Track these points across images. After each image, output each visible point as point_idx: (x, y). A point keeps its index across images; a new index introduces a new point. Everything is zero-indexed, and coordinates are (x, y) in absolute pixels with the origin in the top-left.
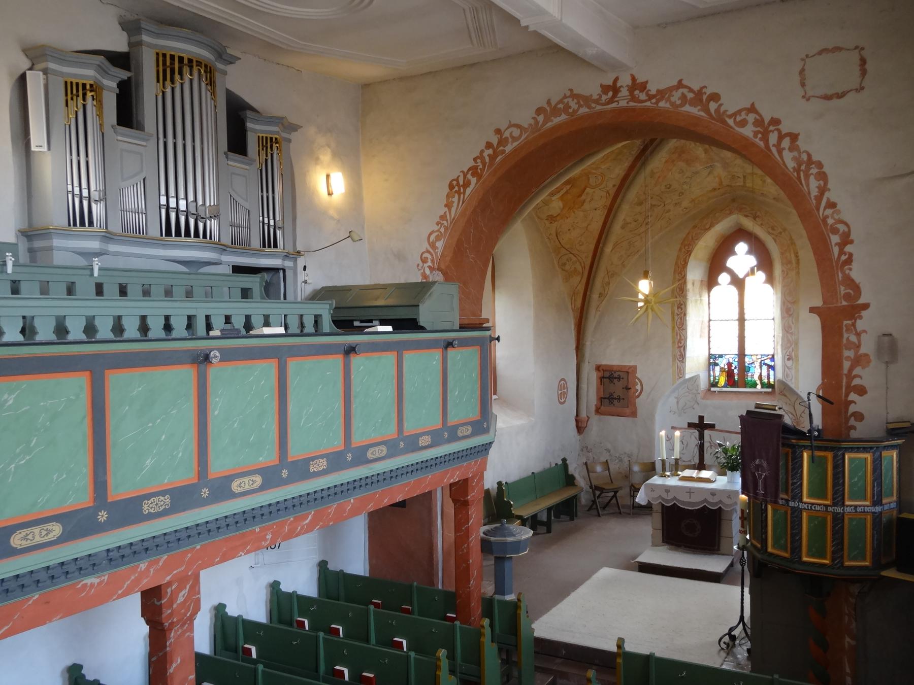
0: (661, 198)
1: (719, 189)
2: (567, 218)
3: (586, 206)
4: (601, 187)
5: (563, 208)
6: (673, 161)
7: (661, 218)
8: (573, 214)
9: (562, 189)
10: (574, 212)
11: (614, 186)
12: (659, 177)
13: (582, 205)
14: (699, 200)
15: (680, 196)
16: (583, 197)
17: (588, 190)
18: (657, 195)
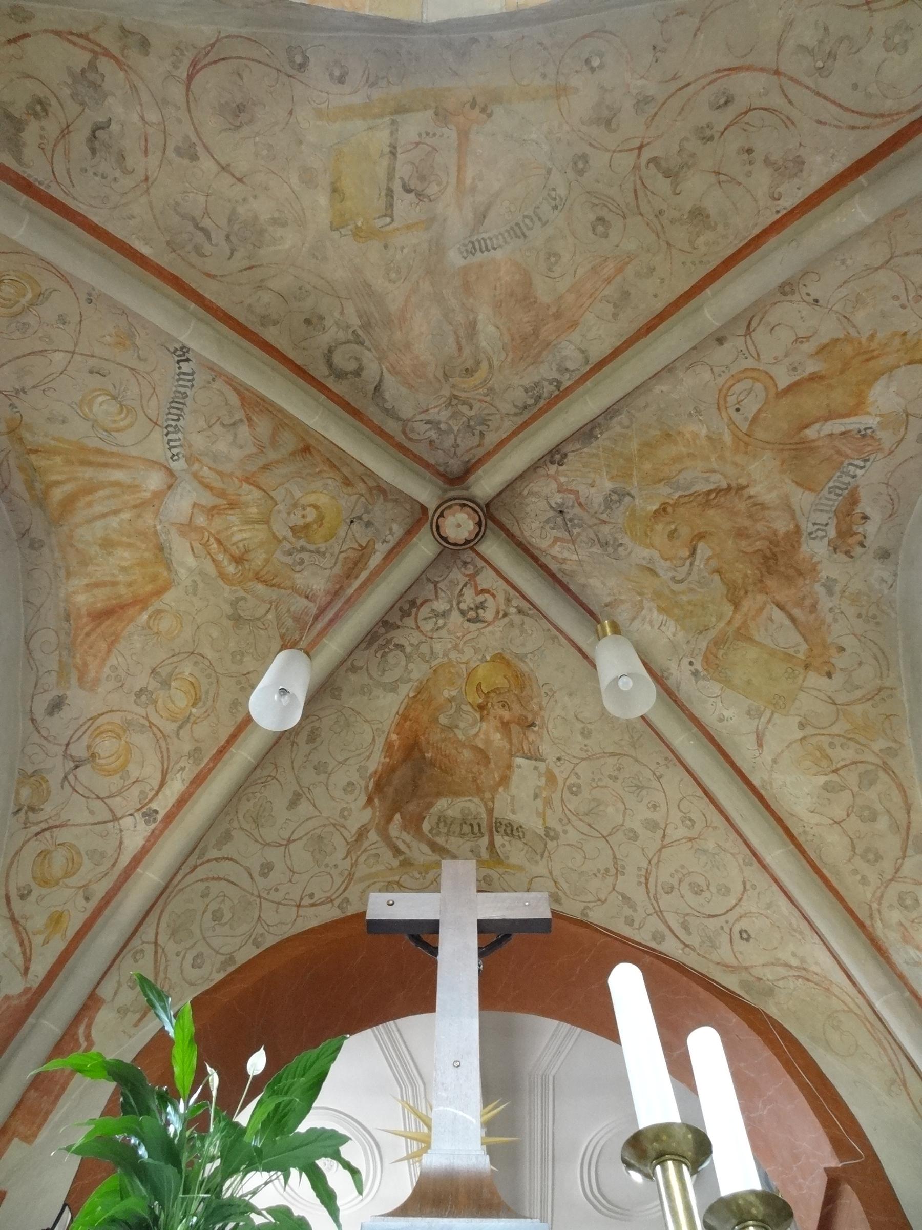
0: (636, 195)
1: (473, 105)
2: (905, 334)
3: (829, 329)
4: (750, 363)
5: (883, 374)
6: (557, 316)
7: (681, 83)
8: (878, 334)
9: (831, 435)
10: (872, 337)
11: (720, 341)
12: (609, 281)
13: (838, 340)
14: (544, 76)
15: (584, 157)
16: (812, 367)
17: (782, 385)
18: (641, 214)
